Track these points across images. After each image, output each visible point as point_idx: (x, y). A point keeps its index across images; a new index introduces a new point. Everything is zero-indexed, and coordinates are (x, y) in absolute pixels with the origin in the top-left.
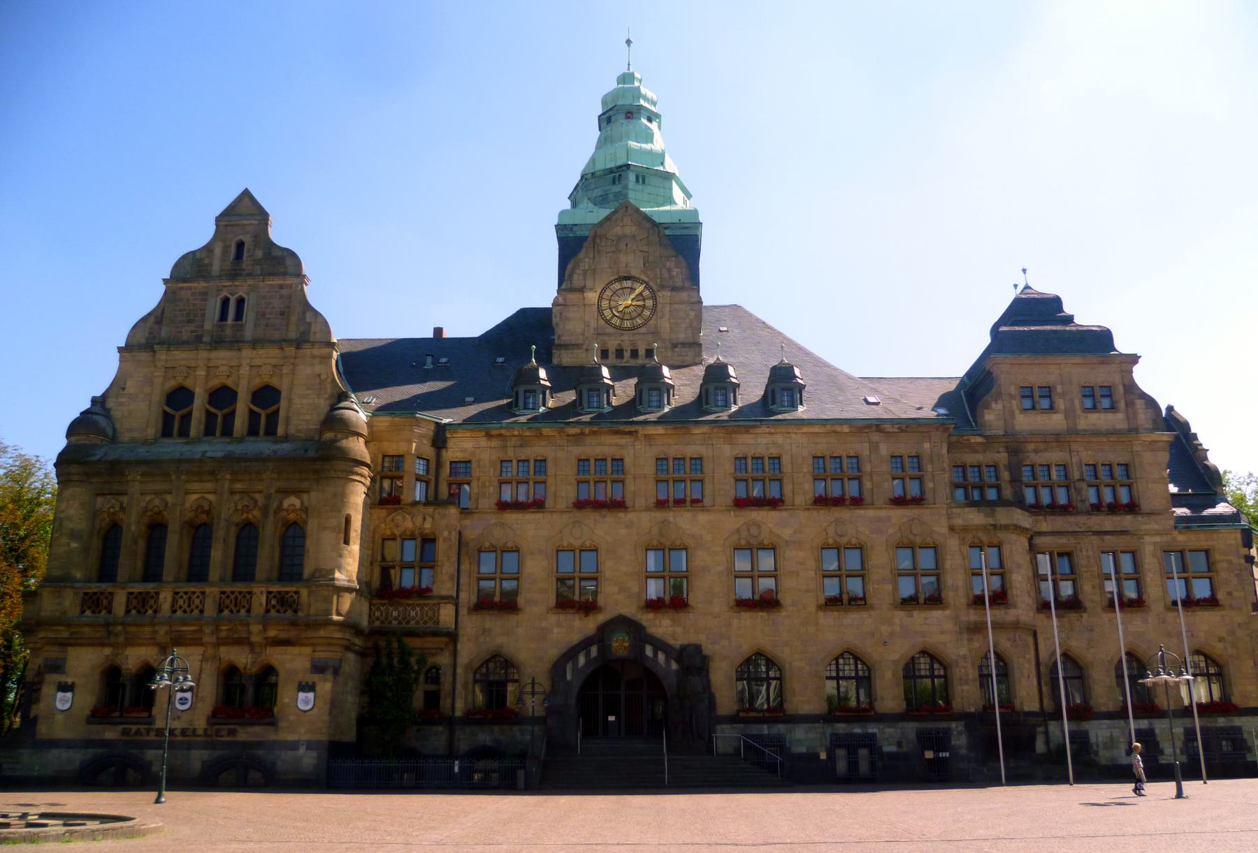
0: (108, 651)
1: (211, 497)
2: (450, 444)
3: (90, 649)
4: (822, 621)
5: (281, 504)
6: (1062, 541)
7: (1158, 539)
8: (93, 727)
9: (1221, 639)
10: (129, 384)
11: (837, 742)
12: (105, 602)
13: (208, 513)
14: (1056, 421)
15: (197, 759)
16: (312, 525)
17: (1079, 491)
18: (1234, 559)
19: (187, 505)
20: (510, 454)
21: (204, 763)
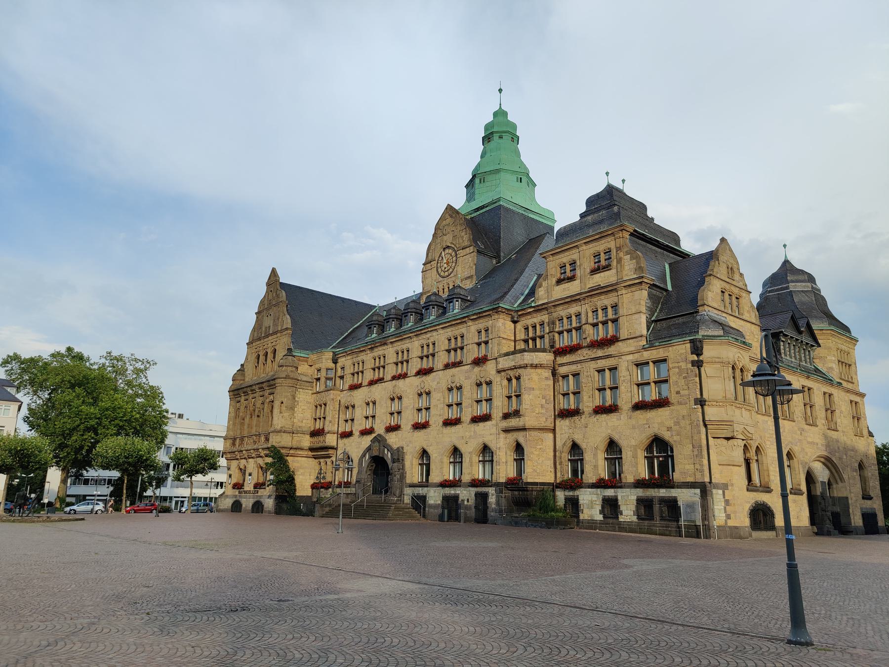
7: (630, 357)
14: (574, 288)
18: (683, 365)
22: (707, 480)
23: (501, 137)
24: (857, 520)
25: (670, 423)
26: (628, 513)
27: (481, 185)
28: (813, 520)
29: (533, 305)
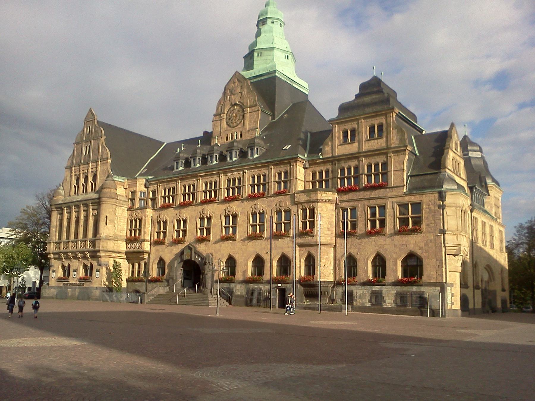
7: (395, 200)
9: (421, 248)
22: (444, 281)
23: (273, 23)
24: (499, 305)
25: (422, 245)
26: (389, 302)
27: (259, 58)
28: (483, 304)
29: (321, 157)
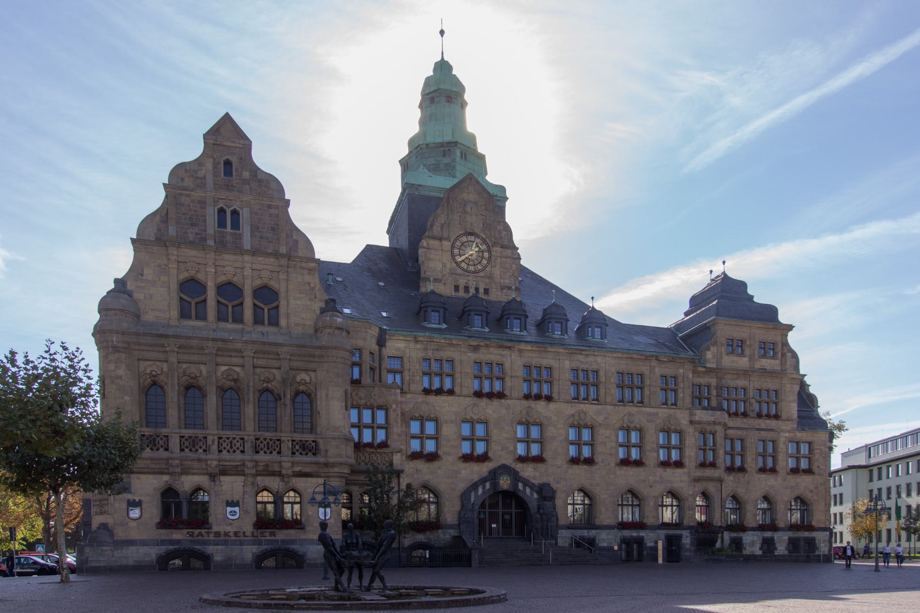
0: (166, 478)
1: (238, 369)
2: (388, 344)
3: (151, 477)
4: (618, 472)
5: (295, 377)
6: (739, 432)
7: (787, 435)
8: (162, 531)
10: (146, 272)
11: (625, 541)
12: (161, 443)
13: (235, 380)
15: (249, 552)
16: (321, 394)
17: (751, 405)
18: (823, 448)
19: (219, 374)
20: (430, 354)
21: (253, 554)
26: (781, 549)
